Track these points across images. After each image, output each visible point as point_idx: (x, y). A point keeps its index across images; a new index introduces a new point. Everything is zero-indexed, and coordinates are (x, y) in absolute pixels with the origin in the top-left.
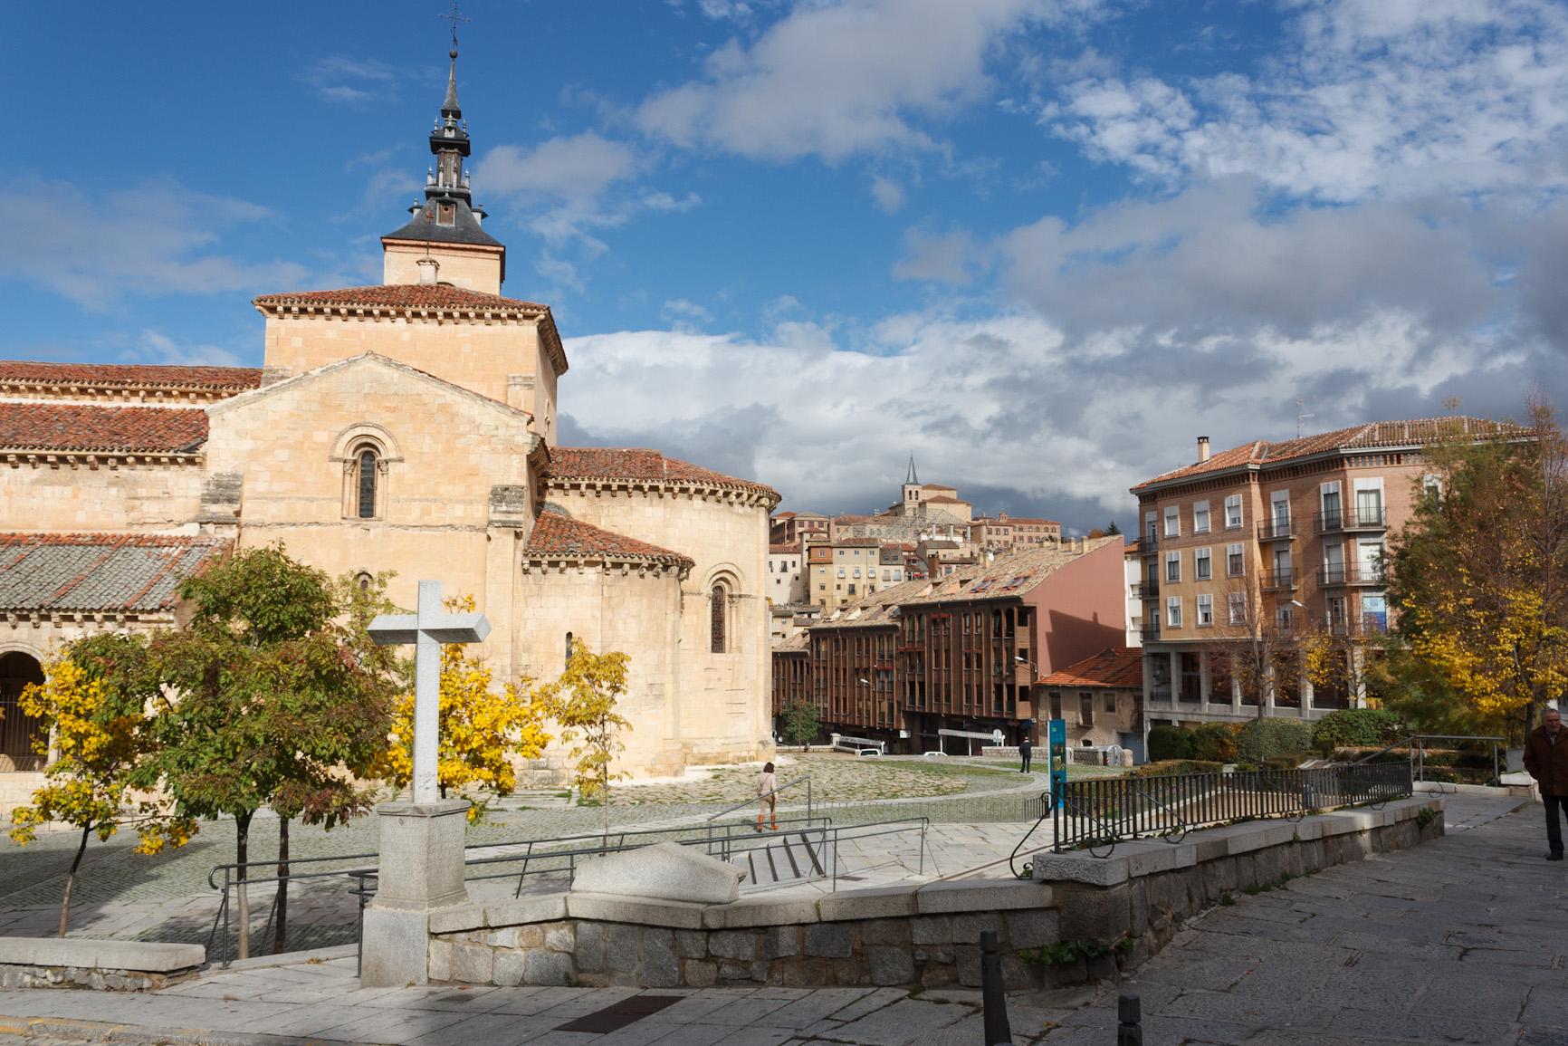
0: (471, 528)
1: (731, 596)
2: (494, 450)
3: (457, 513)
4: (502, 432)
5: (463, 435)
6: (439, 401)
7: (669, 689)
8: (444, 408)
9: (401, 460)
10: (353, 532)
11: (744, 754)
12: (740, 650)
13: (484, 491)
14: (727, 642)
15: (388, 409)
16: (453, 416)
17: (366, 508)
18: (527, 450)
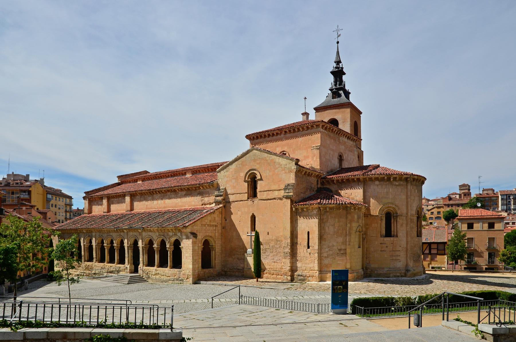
0: (280, 199)
1: (394, 216)
2: (286, 173)
3: (276, 194)
4: (288, 166)
5: (277, 168)
6: (271, 158)
7: (348, 251)
8: (272, 160)
9: (261, 179)
10: (250, 202)
11: (398, 274)
12: (397, 236)
13: (283, 187)
14: (393, 233)
15: (258, 164)
16: (275, 163)
17: (255, 195)
18: (295, 170)
